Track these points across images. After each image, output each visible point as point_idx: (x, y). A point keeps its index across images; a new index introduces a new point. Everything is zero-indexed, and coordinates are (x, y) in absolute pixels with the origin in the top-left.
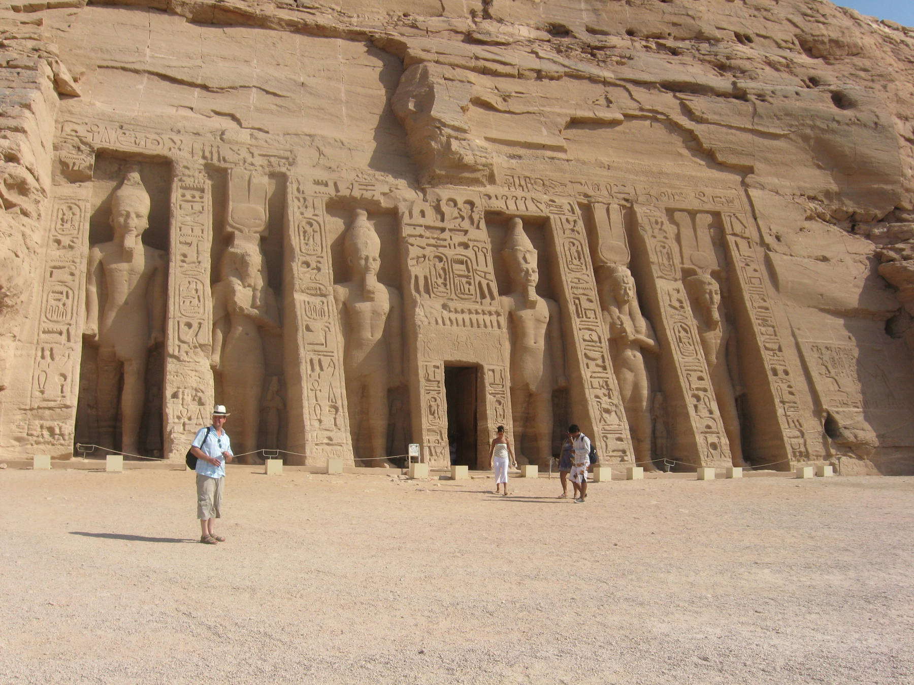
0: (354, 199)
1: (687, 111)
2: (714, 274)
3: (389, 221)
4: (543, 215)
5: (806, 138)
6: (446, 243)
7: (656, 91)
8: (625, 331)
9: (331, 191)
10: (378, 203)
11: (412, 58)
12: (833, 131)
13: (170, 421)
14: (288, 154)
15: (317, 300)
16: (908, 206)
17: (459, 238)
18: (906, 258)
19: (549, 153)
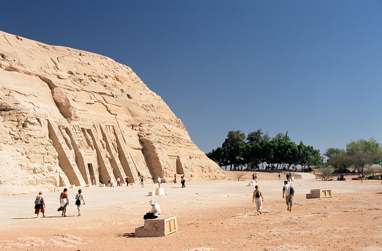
0: (61, 126)
1: (105, 100)
2: (115, 141)
3: (67, 130)
4: (90, 129)
5: (125, 107)
6: (78, 136)
7: (98, 94)
8: (107, 155)
9: (57, 123)
10: (64, 127)
11: (55, 86)
12: (130, 105)
13: (62, 178)
14: (45, 114)
15: (67, 151)
16: (143, 123)
17: (80, 135)
18: (145, 136)
19: (85, 112)
